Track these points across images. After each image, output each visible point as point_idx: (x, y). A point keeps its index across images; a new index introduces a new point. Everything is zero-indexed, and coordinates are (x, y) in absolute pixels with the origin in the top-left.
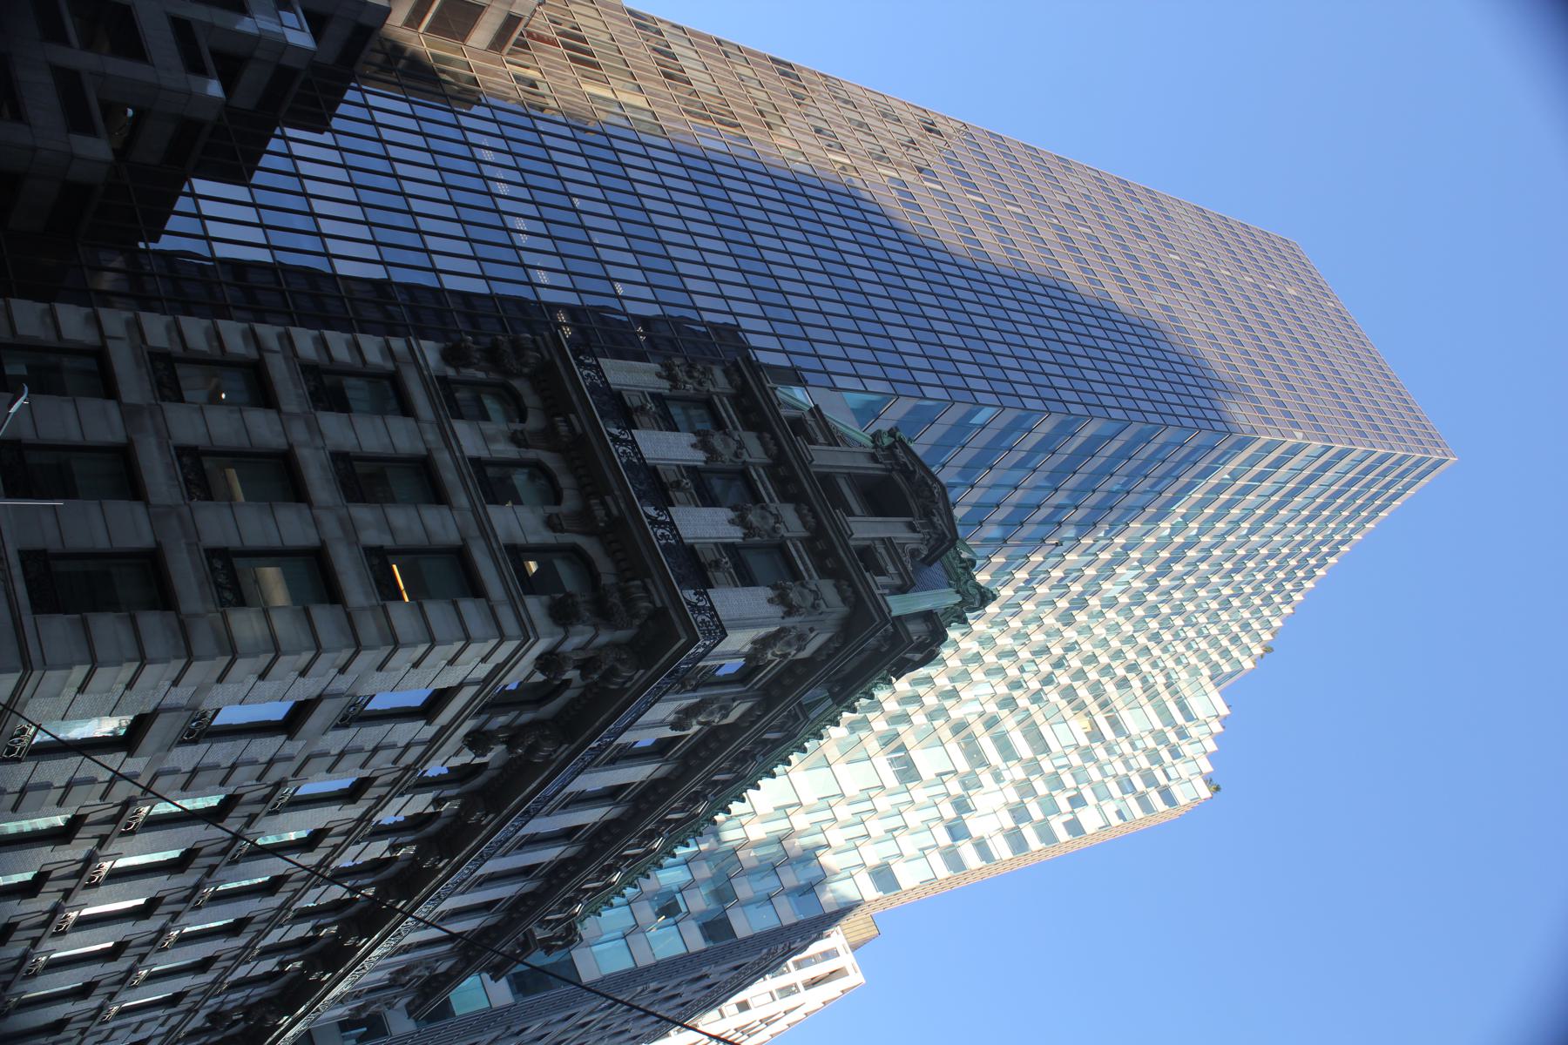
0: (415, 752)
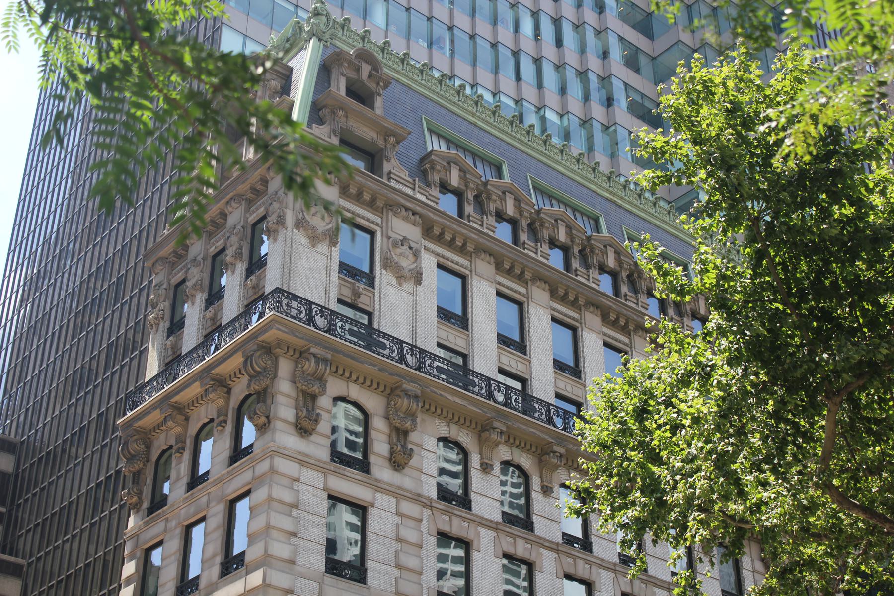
0: (408, 507)
